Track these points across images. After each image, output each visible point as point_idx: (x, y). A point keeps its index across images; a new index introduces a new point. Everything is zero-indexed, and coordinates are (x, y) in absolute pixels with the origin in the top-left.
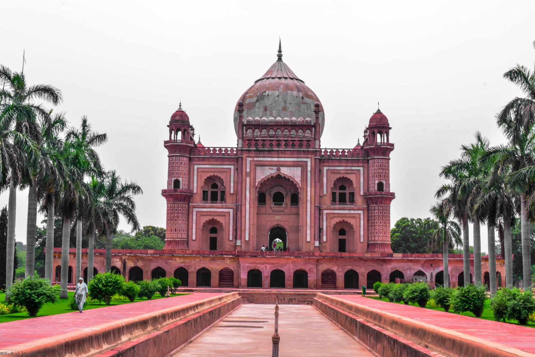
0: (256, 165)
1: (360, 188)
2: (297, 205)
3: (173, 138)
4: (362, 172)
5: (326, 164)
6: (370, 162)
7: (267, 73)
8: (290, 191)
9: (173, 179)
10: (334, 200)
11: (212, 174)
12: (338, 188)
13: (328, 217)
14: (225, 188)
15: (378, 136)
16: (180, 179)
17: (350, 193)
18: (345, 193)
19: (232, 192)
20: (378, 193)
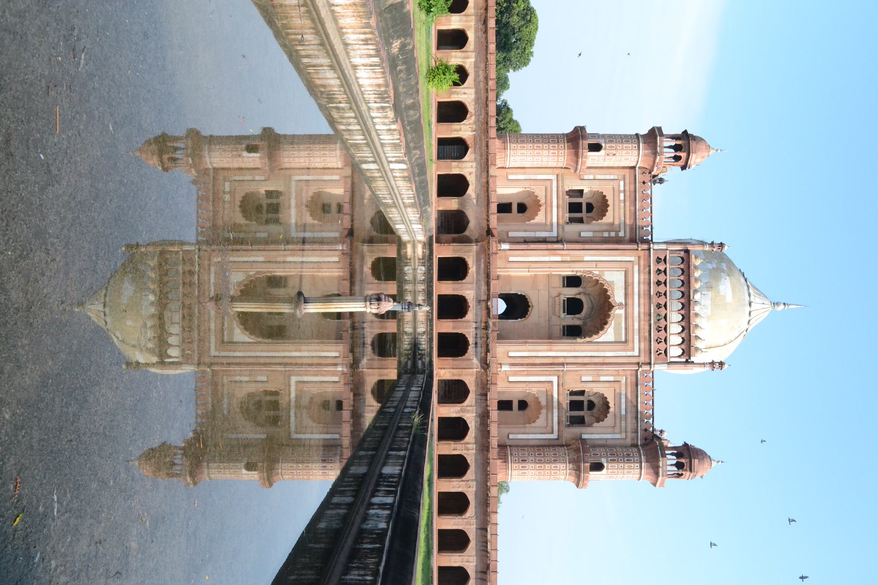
0: (626, 271)
1: (594, 433)
2: (564, 335)
4: (618, 436)
5: (629, 381)
7: (754, 287)
8: (585, 324)
11: (610, 202)
13: (546, 384)
14: (588, 223)
15: (674, 462)
16: (602, 152)
17: (583, 417)
18: (582, 410)
19: (583, 234)
20: (588, 465)
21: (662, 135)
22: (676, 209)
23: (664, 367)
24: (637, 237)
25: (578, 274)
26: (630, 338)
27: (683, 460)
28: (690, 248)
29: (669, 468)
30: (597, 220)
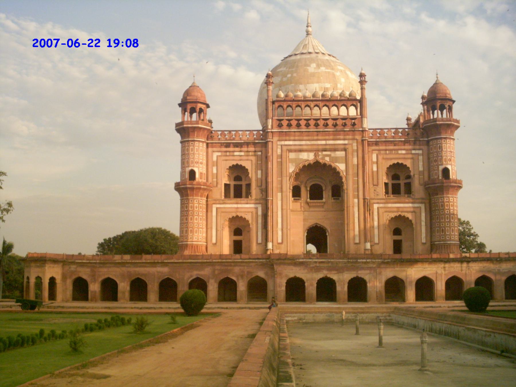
3: (186, 119)
6: (431, 143)
7: (296, 49)
9: (188, 169)
10: (387, 193)
11: (235, 163)
12: (390, 178)
16: (196, 170)
17: (405, 183)
18: (399, 184)
20: (444, 181)
21: (182, 123)
22: (236, 110)
23: (365, 121)
24: (261, 142)
25: (292, 188)
26: (342, 147)
27: (438, 105)
28: (270, 100)
29: (445, 116)
30: (248, 173)
